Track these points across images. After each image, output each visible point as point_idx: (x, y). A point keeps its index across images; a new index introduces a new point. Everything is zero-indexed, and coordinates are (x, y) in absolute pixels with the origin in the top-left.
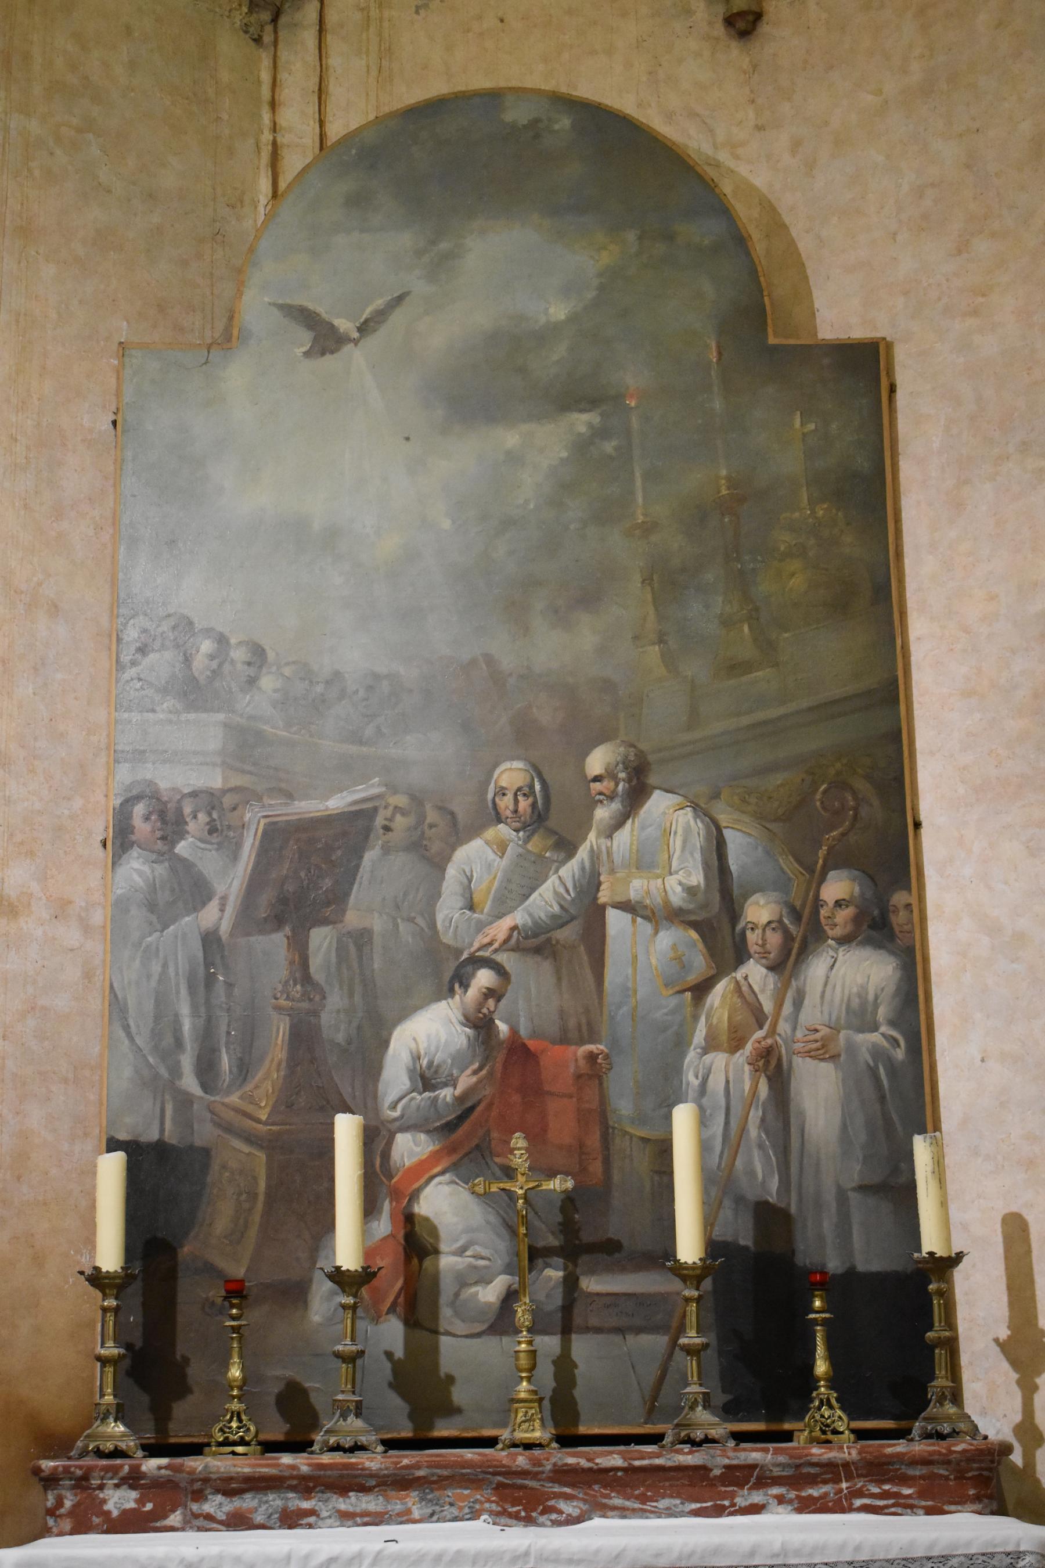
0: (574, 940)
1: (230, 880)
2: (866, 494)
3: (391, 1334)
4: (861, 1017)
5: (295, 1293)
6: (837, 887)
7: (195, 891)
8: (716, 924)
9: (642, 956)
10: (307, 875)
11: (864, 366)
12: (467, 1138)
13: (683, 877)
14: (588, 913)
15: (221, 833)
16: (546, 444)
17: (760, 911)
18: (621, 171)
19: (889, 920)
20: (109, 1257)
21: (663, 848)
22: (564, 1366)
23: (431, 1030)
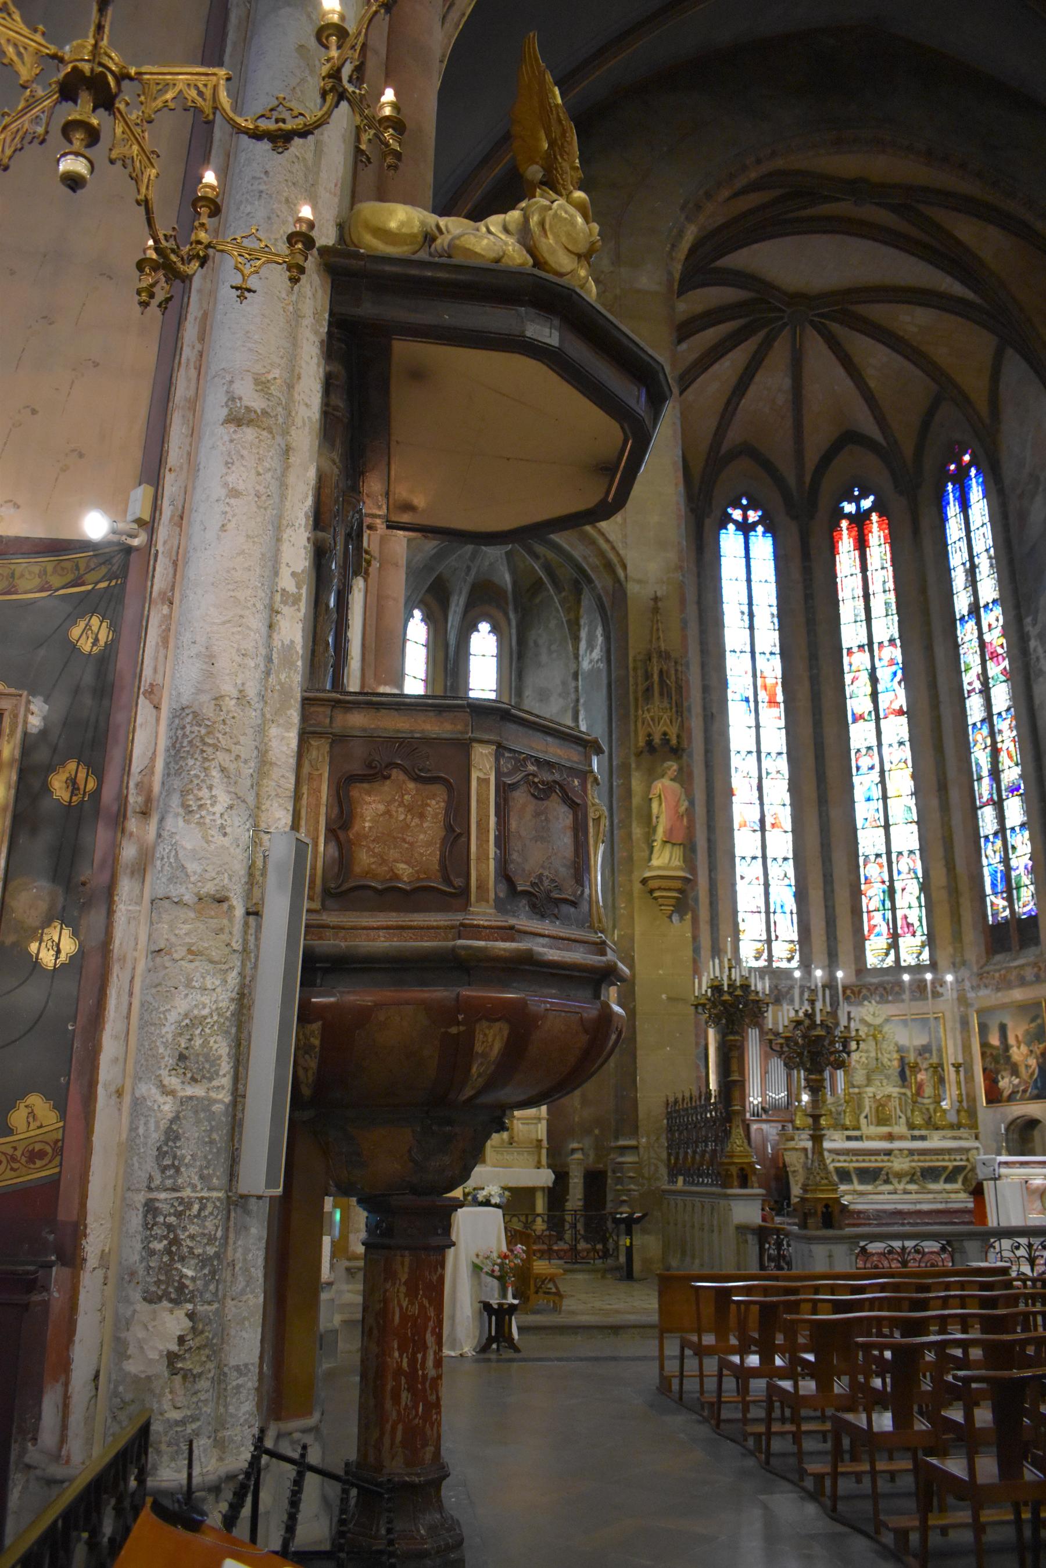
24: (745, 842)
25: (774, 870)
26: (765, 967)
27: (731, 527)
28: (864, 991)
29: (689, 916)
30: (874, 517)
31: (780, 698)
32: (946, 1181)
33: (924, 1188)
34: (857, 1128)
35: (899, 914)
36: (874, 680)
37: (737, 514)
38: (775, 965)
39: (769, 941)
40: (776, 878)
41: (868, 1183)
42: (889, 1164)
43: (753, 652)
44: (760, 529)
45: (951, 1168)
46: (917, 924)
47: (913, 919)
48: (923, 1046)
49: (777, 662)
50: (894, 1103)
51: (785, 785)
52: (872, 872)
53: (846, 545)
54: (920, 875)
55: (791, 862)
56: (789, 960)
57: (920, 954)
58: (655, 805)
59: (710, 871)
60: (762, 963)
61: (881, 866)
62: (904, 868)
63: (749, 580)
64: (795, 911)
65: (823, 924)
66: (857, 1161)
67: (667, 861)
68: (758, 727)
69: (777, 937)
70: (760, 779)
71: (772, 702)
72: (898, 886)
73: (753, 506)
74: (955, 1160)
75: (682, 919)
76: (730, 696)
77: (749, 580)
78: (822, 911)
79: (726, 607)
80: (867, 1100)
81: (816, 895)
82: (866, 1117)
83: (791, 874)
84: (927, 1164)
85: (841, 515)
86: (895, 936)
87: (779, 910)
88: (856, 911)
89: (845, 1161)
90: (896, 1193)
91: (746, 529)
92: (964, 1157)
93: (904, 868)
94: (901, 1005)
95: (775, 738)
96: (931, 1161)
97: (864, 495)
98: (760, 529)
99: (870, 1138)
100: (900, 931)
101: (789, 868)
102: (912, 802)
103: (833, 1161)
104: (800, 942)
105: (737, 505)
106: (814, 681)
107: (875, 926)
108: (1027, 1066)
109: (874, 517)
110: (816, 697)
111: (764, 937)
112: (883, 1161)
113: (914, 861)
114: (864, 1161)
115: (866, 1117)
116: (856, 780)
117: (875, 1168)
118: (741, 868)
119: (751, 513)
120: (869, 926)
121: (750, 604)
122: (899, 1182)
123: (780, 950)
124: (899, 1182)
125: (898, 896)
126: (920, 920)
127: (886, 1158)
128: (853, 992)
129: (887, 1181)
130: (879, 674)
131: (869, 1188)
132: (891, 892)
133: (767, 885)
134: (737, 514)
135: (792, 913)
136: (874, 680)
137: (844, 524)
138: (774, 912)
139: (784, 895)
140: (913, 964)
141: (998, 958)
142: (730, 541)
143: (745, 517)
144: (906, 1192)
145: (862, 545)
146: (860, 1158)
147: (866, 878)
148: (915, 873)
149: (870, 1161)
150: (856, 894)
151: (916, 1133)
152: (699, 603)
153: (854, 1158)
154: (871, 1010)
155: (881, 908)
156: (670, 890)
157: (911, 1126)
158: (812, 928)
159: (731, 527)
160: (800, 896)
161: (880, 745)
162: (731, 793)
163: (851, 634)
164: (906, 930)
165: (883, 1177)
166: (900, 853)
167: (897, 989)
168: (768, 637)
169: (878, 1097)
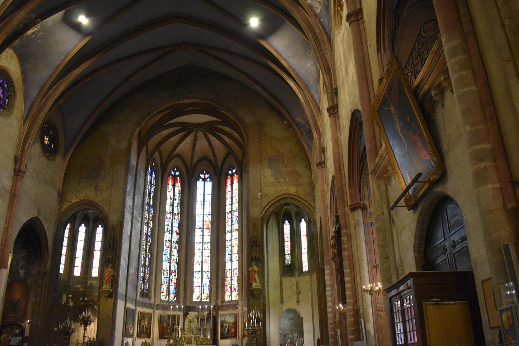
0: (293, 338)
2: (302, 323)
8: (297, 337)
9: (295, 338)
10: (285, 336)
11: (302, 318)
16: (292, 321)
18: (294, 311)
19: (303, 337)
21: (296, 335)
23: (289, 341)
24: (197, 268)
25: (204, 275)
27: (201, 180)
30: (235, 175)
31: (210, 227)
35: (233, 286)
36: (232, 221)
37: (202, 176)
39: (201, 294)
43: (203, 215)
44: (209, 179)
47: (236, 287)
49: (210, 217)
51: (209, 251)
52: (228, 274)
53: (229, 183)
60: (199, 300)
62: (235, 273)
63: (204, 195)
65: (215, 289)
68: (203, 235)
70: (202, 250)
71: (208, 228)
72: (233, 278)
73: (207, 173)
76: (196, 227)
77: (204, 195)
78: (215, 286)
79: (197, 203)
81: (214, 281)
83: (209, 275)
85: (228, 174)
86: (231, 292)
88: (224, 286)
91: (204, 180)
95: (207, 238)
97: (233, 169)
98: (209, 179)
101: (209, 274)
102: (237, 255)
105: (202, 173)
106: (218, 222)
109: (235, 175)
110: (218, 226)
116: (226, 249)
119: (206, 175)
121: (204, 201)
123: (204, 296)
130: (233, 219)
132: (231, 280)
133: (202, 279)
134: (202, 176)
136: (232, 221)
137: (229, 177)
139: (206, 281)
142: (200, 184)
143: (205, 176)
145: (232, 183)
150: (224, 280)
152: (188, 203)
159: (201, 180)
160: (210, 282)
161: (232, 239)
162: (194, 254)
163: (228, 209)
168: (208, 210)
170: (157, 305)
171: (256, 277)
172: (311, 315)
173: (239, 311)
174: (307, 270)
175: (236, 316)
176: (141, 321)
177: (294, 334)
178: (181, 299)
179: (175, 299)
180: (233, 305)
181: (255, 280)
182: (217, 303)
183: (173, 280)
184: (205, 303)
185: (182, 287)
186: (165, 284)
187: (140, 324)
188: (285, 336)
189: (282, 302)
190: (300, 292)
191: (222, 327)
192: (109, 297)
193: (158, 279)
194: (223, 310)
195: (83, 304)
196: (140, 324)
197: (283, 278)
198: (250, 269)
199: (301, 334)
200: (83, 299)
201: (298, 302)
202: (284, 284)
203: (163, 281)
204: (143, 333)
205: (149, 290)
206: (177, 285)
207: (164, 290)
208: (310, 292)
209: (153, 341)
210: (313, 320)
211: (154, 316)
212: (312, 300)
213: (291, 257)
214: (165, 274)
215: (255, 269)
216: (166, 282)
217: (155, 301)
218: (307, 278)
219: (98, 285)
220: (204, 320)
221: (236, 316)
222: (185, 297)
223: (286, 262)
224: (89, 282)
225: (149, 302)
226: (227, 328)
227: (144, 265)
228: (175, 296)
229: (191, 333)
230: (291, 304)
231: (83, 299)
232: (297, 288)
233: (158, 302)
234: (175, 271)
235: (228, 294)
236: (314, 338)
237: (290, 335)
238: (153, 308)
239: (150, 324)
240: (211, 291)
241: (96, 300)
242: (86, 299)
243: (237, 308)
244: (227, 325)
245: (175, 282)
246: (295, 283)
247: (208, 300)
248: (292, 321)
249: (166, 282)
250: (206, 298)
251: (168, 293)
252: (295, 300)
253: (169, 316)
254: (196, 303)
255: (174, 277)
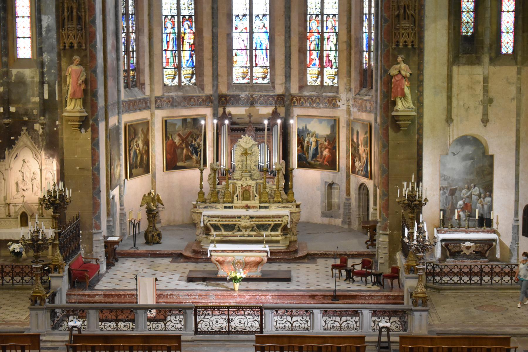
0: (470, 197)
1: (448, 192)
2: (491, 166)
3: (458, 221)
4: (489, 202)
5: (452, 219)
6: (488, 193)
7: (445, 193)
8: (479, 196)
9: (474, 198)
10: (453, 192)
11: (492, 157)
12: (463, 209)
13: (477, 193)
14: (471, 195)
15: (447, 189)
16: (469, 162)
17: (482, 195)
19: (491, 196)
20: (442, 218)
21: (476, 191)
22: (468, 223)
23: (461, 202)
25: (257, 23)
26: (248, 83)
28: (302, 100)
29: (90, 130)
32: (272, 230)
33: (260, 234)
34: (232, 202)
35: (325, 53)
38: (254, 81)
39: (251, 67)
40: (257, 28)
41: (230, 231)
42: (239, 223)
45: (273, 225)
46: (333, 61)
47: (332, 58)
48: (327, 135)
50: (253, 190)
54: (337, 31)
55: (268, 17)
56: (263, 78)
57: (334, 79)
58: (68, 79)
59: (213, 27)
60: (246, 81)
61: (318, 23)
62: (329, 25)
64: (268, 48)
65: (283, 57)
66: (222, 221)
67: (72, 108)
69: (256, 64)
72: (326, 36)
74: (275, 221)
75: (86, 131)
80: (238, 188)
81: (280, 40)
82: (237, 196)
83: (267, 24)
84: (260, 223)
87: (258, 48)
88: (303, 51)
89: (216, 221)
90: (244, 236)
92: (280, 219)
93: (329, 25)
94: (319, 110)
96: (262, 221)
99: (236, 207)
100: (325, 64)
101: (267, 22)
103: (209, 221)
104: (270, 67)
107: (313, 59)
108: (363, 158)
111: (248, 65)
112: (236, 221)
113: (335, 21)
114: (226, 221)
115: (237, 196)
117: (232, 224)
118: (236, 22)
120: (310, 59)
122: (246, 231)
123: (258, 72)
124: (246, 231)
125: (325, 42)
126: (335, 59)
127: (237, 219)
128: (297, 100)
129: (239, 230)
131: (230, 233)
132: (322, 40)
133: (251, 33)
135: (266, 49)
138: (256, 49)
139: (262, 38)
140: (330, 85)
141: (364, 91)
144: (249, 236)
146: (224, 219)
147: (310, 29)
148: (335, 29)
149: (229, 221)
150: (303, 38)
151: (263, 205)
153: (221, 220)
154: (245, 140)
155: (317, 49)
156: (74, 121)
157: (261, 202)
158: (276, 60)
160: (271, 39)
164: (328, 64)
165: (236, 228)
166: (328, 15)
167: (318, 100)
169: (244, 186)
170: (157, 99)
171: (407, 91)
172: (514, 152)
173: (341, 113)
174: (510, 52)
175: (335, 124)
176: (130, 142)
177: (473, 190)
178: (208, 79)
179: (193, 80)
180: (327, 97)
181: (404, 96)
182: (287, 89)
183: (186, 36)
184: (260, 87)
185: (207, 54)
186: (170, 48)
187: (130, 150)
188: (453, 192)
189: (449, 120)
190: (491, 101)
191: (300, 143)
192: (80, 127)
193: (155, 40)
194: (302, 106)
195: (6, 121)
196: (130, 150)
197: (455, 68)
198: (393, 71)
199: (488, 189)
200: (6, 110)
201: (485, 121)
202: (455, 81)
203: (165, 43)
204: (136, 167)
205: (137, 69)
206: (196, 48)
207: (168, 63)
208: (514, 103)
209: (154, 176)
210: (517, 165)
211: (153, 123)
212: (518, 122)
213: (476, 18)
214: (169, 25)
215: (403, 73)
216: (171, 43)
217: (152, 90)
218: (511, 71)
219: (37, 79)
220: (263, 130)
221: (335, 124)
222: (215, 76)
223: (464, 31)
224: (14, 71)
225: (141, 96)
226: (313, 147)
227: (126, 14)
228: (193, 74)
229: (248, 178)
230: (471, 126)
231: (6, 110)
232: (486, 90)
233: (158, 92)
234: (190, 17)
235: (312, 71)
236: (517, 201)
237: (464, 191)
238: (149, 108)
239: (147, 143)
240: (272, 61)
241: (35, 112)
242: (12, 109)
243: (335, 106)
244: (313, 139)
245: (192, 41)
246: (481, 79)
247: (266, 81)
248: (469, 162)
249: (171, 43)
250: (261, 75)
251: (179, 68)
252: (480, 116)
253: (184, 121)
254: (241, 87)
255: (188, 31)
